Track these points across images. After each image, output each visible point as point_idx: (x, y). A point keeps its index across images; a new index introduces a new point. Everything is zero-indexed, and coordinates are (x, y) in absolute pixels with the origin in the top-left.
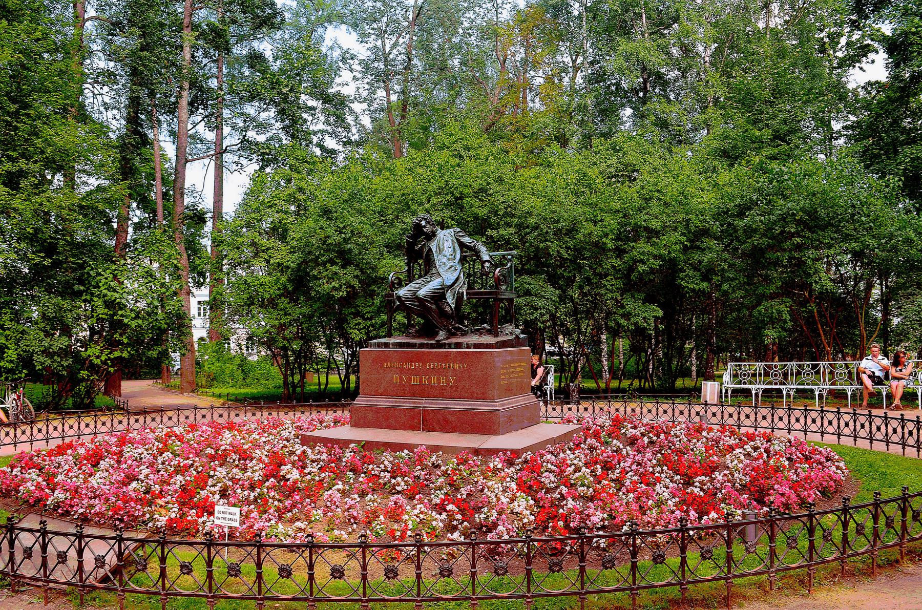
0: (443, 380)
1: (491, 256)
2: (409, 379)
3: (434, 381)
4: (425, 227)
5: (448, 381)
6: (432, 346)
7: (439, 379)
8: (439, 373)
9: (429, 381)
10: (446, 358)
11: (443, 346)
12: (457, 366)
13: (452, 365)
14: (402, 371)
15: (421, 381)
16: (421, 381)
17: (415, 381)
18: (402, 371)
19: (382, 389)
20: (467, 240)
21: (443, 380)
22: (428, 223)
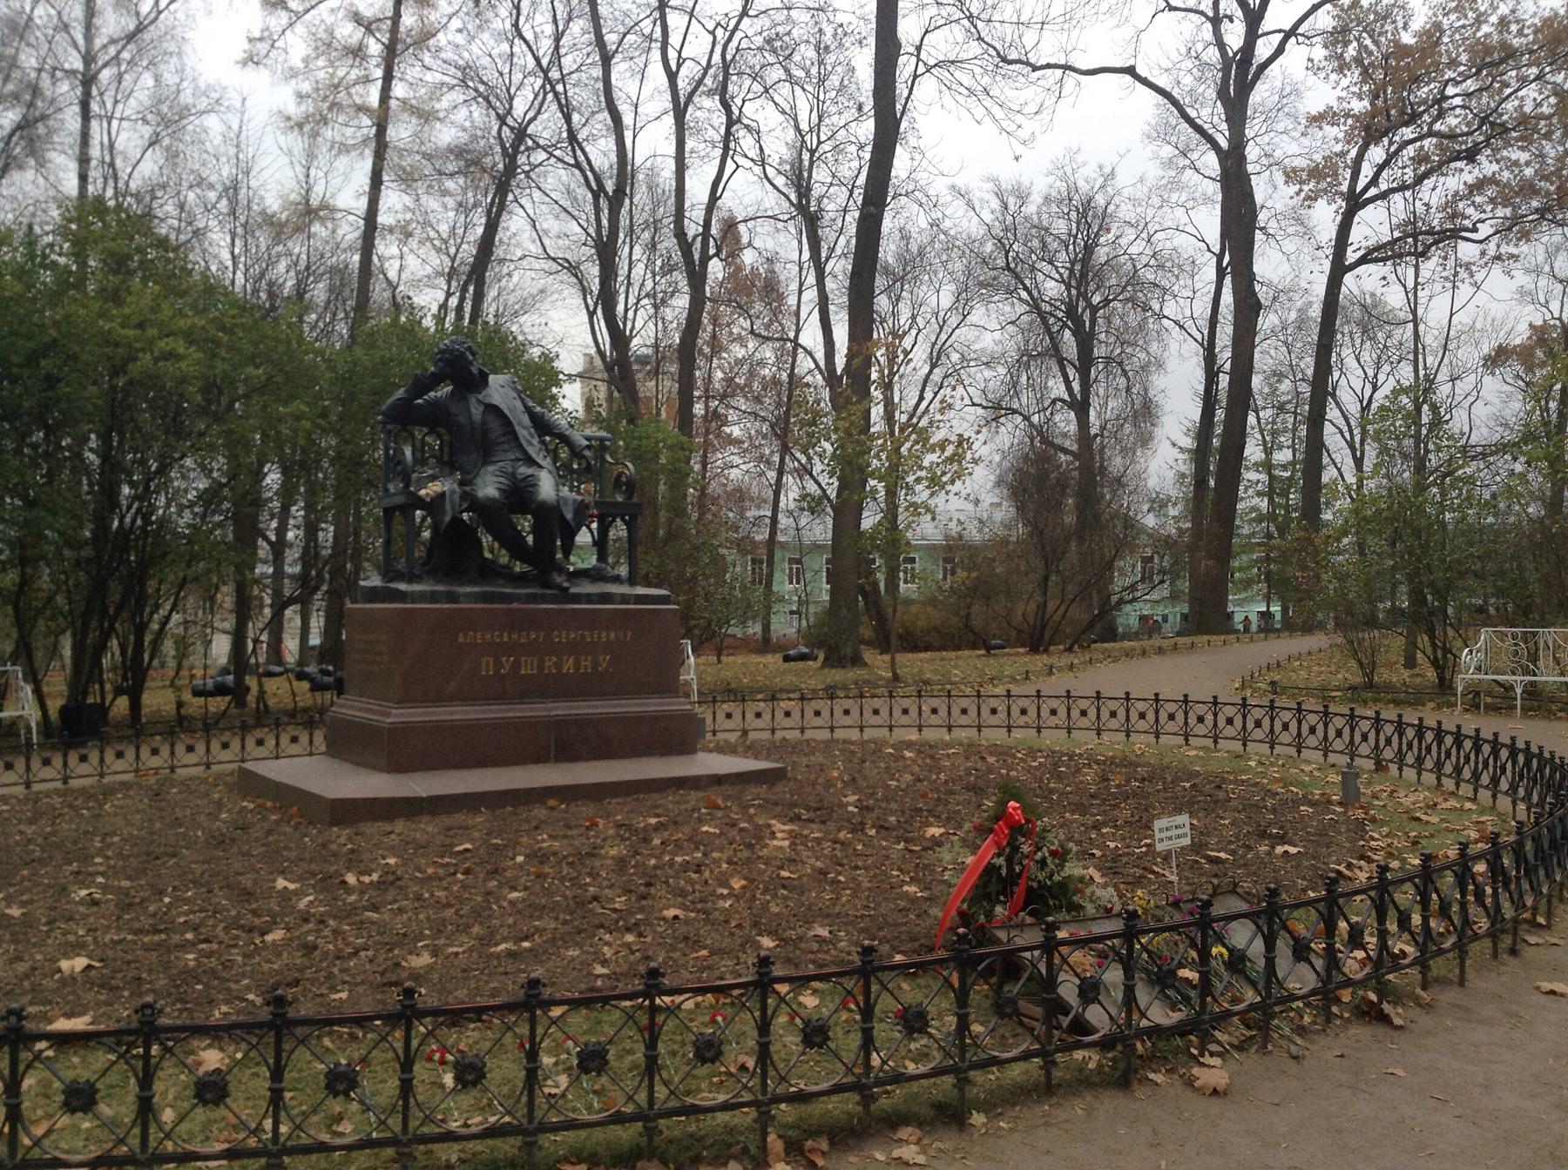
0: (586, 663)
2: (516, 666)
3: (569, 665)
6: (553, 600)
9: (558, 665)
11: (577, 598)
12: (613, 635)
13: (604, 634)
15: (541, 667)
16: (541, 667)
21: (586, 663)
22: (473, 354)
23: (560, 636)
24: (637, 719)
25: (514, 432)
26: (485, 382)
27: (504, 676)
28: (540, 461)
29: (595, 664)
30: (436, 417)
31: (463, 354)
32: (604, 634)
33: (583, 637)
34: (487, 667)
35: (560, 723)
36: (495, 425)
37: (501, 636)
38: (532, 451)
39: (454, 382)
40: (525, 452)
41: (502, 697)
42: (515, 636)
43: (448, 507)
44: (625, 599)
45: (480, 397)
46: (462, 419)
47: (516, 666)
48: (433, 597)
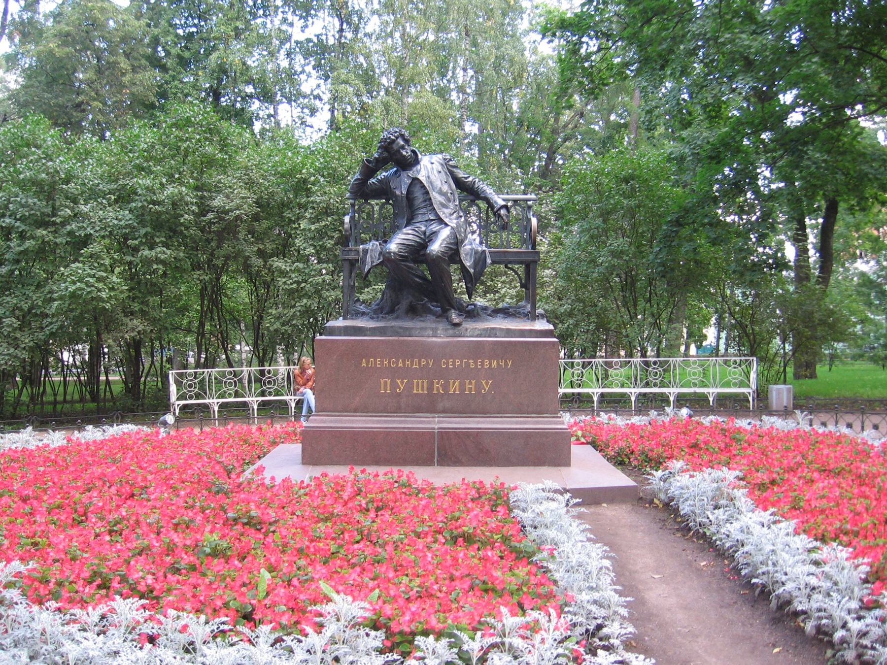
0: (470, 386)
1: (504, 200)
2: (409, 386)
4: (403, 147)
5: (479, 387)
7: (462, 386)
8: (464, 374)
9: (446, 387)
12: (494, 364)
13: (487, 362)
15: (431, 388)
16: (431, 388)
17: (420, 388)
18: (395, 373)
20: (461, 174)
22: (407, 141)
23: (447, 363)
25: (430, 199)
26: (417, 161)
27: (399, 394)
28: (446, 220)
29: (479, 387)
30: (384, 191)
31: (393, 141)
32: (487, 362)
33: (468, 364)
34: (385, 385)
35: (444, 435)
36: (418, 193)
38: (443, 213)
40: (437, 215)
41: (397, 410)
43: (368, 259)
44: (509, 332)
45: (410, 173)
46: (398, 193)
47: (409, 386)
48: (373, 331)
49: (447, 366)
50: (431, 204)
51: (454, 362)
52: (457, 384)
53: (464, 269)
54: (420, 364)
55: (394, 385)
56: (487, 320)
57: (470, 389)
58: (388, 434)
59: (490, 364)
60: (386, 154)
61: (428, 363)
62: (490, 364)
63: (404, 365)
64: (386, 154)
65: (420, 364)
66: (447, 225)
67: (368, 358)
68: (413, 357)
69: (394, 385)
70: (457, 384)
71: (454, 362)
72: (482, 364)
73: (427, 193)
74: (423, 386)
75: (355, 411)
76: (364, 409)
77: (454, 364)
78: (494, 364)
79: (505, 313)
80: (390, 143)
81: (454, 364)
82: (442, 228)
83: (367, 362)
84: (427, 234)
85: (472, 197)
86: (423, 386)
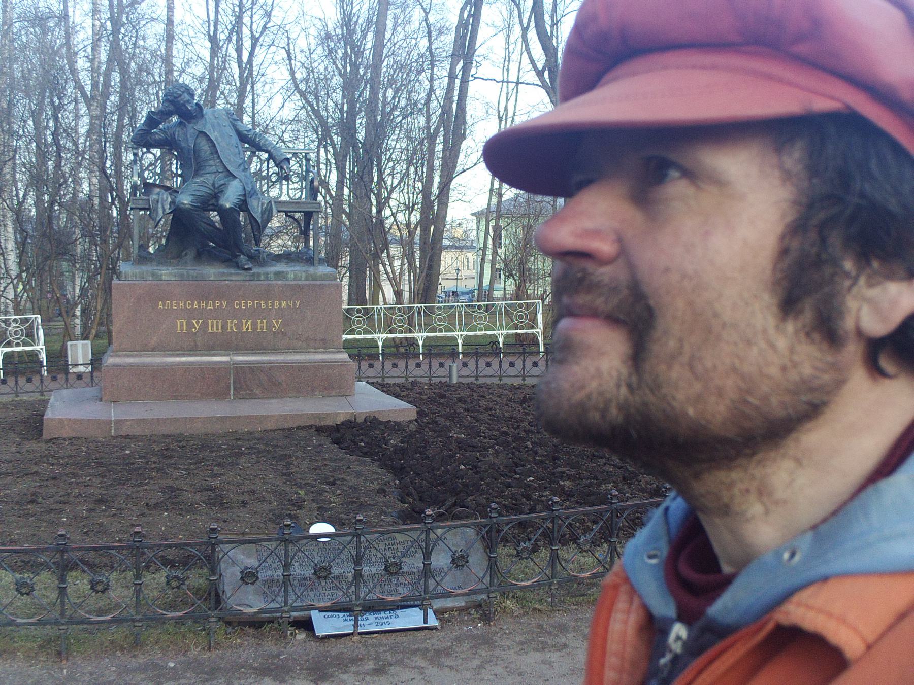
0: (262, 325)
2: (205, 325)
4: (188, 101)
5: (270, 326)
7: (254, 324)
8: (255, 314)
10: (267, 294)
12: (284, 304)
13: (276, 303)
14: (191, 314)
15: (224, 327)
16: (224, 327)
17: (214, 327)
18: (191, 314)
19: (154, 341)
21: (262, 325)
23: (240, 304)
24: (302, 368)
29: (270, 326)
33: (259, 305)
34: (181, 325)
36: (205, 147)
37: (193, 305)
39: (180, 116)
40: (226, 168)
41: (193, 350)
42: (203, 304)
49: (240, 307)
50: (219, 157)
51: (246, 303)
52: (249, 322)
53: (252, 217)
54: (214, 305)
55: (190, 325)
56: (273, 266)
57: (262, 328)
58: (187, 368)
59: (280, 304)
60: (171, 108)
61: (221, 304)
62: (280, 304)
63: (199, 306)
64: (171, 108)
65: (214, 305)
66: (235, 177)
67: (164, 299)
68: (207, 299)
69: (190, 325)
70: (249, 322)
71: (246, 303)
72: (273, 305)
73: (214, 146)
74: (217, 326)
75: (153, 350)
76: (161, 348)
77: (246, 305)
78: (284, 304)
79: (287, 258)
80: (176, 98)
81: (246, 305)
82: (229, 181)
83: (164, 305)
84: (217, 185)
85: (254, 150)
86: (217, 326)
